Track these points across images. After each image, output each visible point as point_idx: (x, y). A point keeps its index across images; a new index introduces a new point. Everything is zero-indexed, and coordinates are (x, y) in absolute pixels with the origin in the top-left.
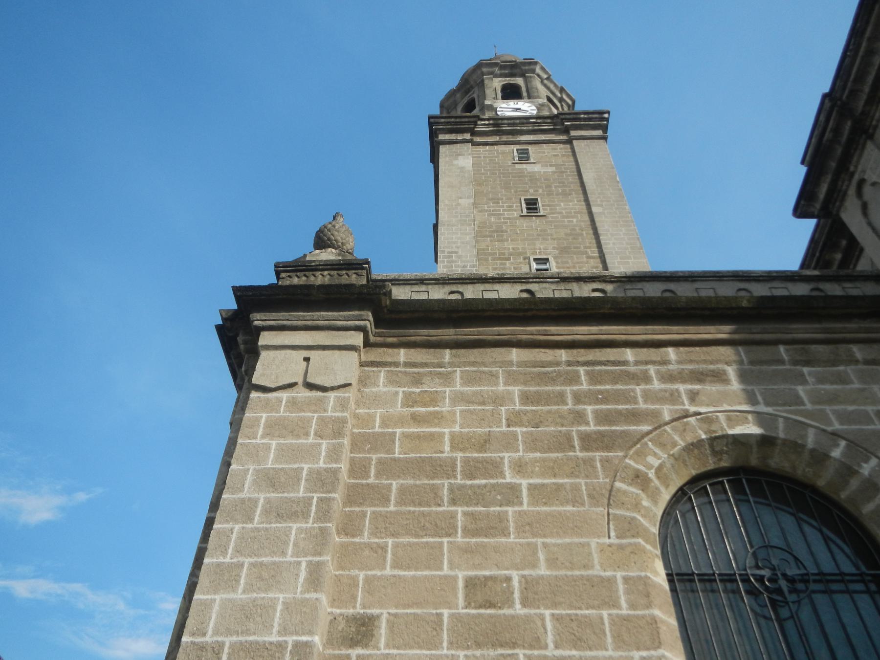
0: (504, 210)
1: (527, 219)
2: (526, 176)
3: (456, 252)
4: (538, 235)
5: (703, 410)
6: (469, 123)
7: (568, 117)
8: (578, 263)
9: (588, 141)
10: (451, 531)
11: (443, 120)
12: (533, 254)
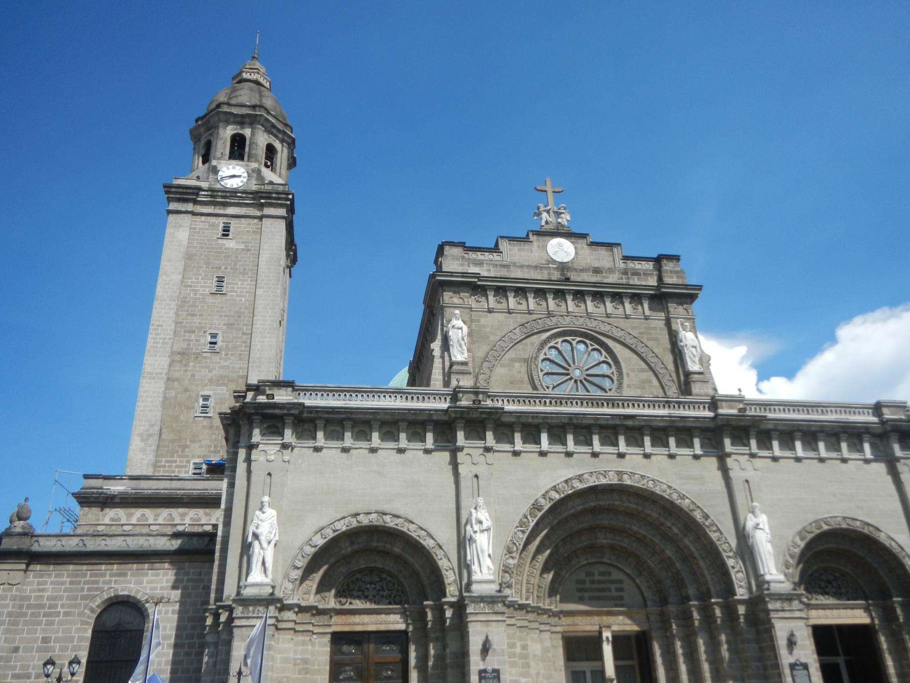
0: (201, 286)
1: (214, 297)
2: (223, 252)
3: (161, 326)
4: (218, 312)
5: (116, 586)
6: (192, 194)
7: (264, 195)
8: (235, 338)
9: (274, 220)
10: (41, 625)
11: (173, 190)
12: (211, 328)
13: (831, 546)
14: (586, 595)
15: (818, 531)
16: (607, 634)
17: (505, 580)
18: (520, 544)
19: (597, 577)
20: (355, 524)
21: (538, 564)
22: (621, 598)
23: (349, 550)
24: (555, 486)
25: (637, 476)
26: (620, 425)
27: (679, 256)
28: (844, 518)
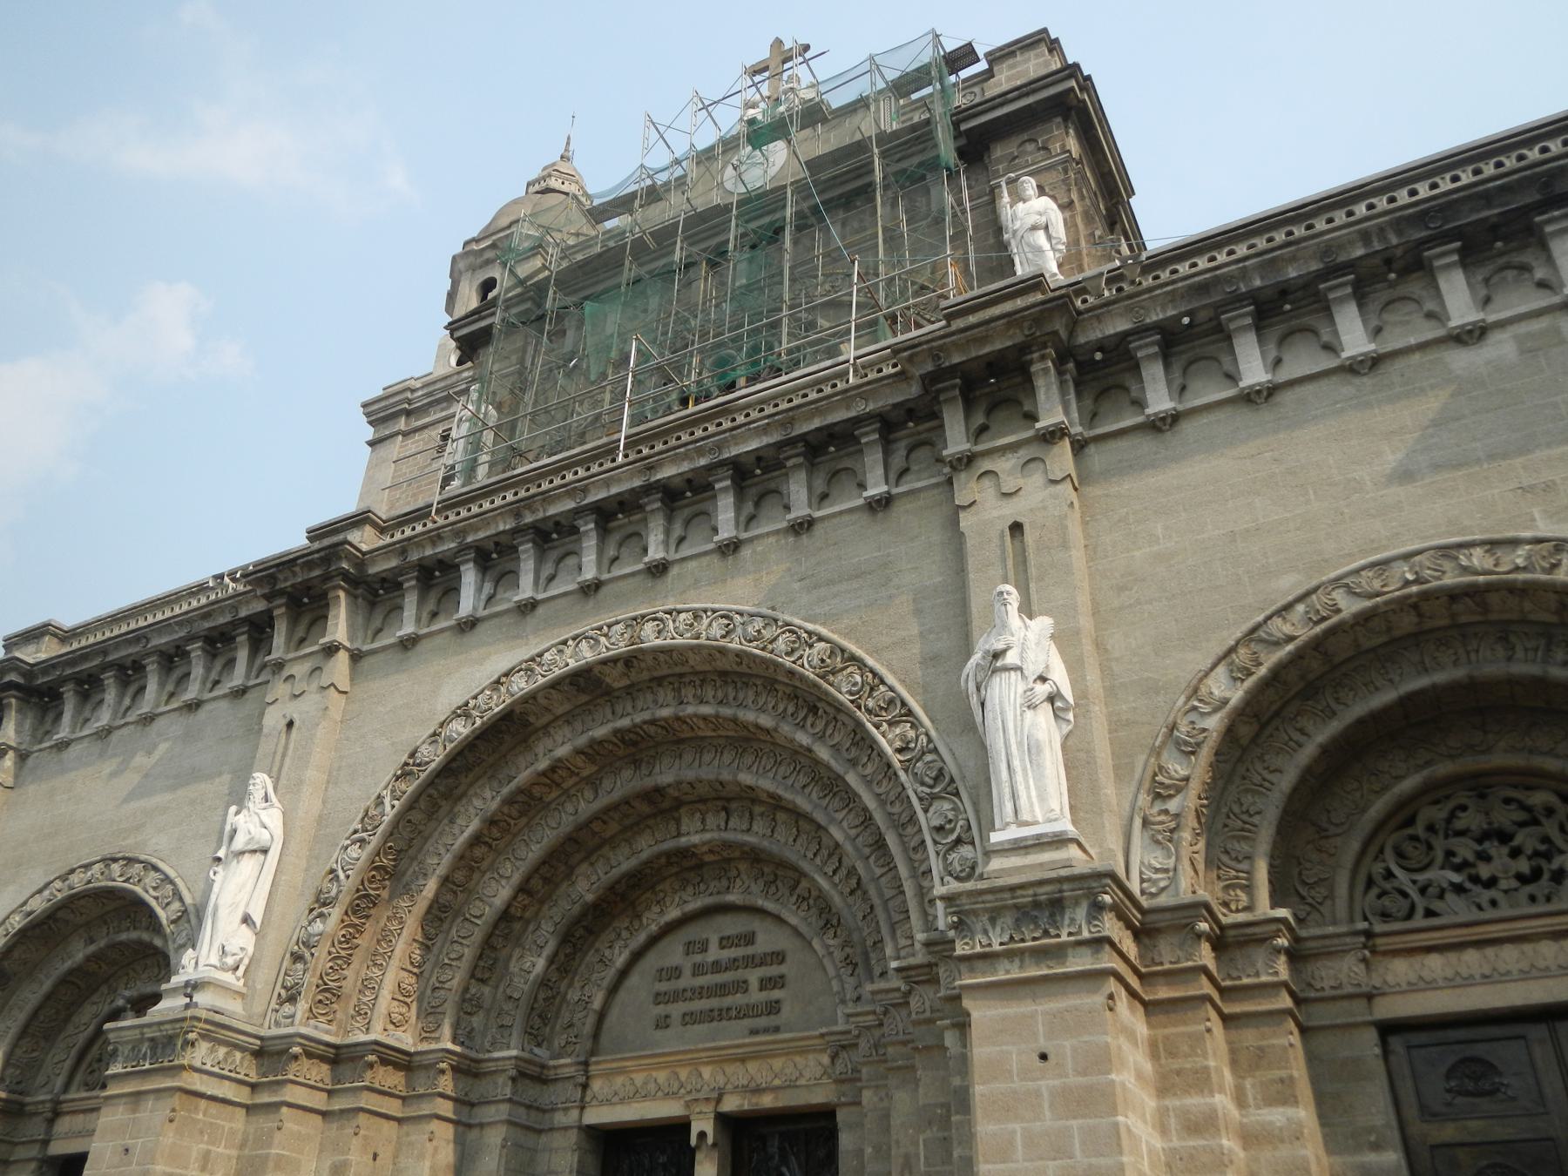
13: (1440, 678)
14: (677, 1010)
15: (1318, 629)
16: (704, 1125)
17: (290, 981)
18: (348, 877)
19: (714, 953)
20: (66, 893)
21: (477, 929)
22: (773, 1008)
23: (79, 957)
24: (466, 704)
25: (683, 616)
26: (648, 489)
27: (1045, 31)
28: (1447, 551)
